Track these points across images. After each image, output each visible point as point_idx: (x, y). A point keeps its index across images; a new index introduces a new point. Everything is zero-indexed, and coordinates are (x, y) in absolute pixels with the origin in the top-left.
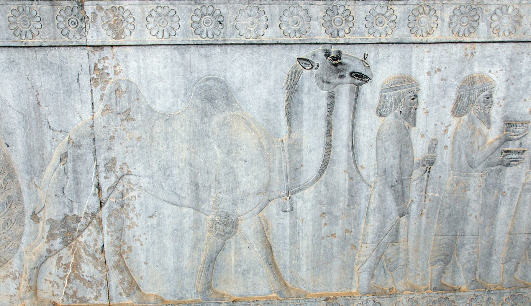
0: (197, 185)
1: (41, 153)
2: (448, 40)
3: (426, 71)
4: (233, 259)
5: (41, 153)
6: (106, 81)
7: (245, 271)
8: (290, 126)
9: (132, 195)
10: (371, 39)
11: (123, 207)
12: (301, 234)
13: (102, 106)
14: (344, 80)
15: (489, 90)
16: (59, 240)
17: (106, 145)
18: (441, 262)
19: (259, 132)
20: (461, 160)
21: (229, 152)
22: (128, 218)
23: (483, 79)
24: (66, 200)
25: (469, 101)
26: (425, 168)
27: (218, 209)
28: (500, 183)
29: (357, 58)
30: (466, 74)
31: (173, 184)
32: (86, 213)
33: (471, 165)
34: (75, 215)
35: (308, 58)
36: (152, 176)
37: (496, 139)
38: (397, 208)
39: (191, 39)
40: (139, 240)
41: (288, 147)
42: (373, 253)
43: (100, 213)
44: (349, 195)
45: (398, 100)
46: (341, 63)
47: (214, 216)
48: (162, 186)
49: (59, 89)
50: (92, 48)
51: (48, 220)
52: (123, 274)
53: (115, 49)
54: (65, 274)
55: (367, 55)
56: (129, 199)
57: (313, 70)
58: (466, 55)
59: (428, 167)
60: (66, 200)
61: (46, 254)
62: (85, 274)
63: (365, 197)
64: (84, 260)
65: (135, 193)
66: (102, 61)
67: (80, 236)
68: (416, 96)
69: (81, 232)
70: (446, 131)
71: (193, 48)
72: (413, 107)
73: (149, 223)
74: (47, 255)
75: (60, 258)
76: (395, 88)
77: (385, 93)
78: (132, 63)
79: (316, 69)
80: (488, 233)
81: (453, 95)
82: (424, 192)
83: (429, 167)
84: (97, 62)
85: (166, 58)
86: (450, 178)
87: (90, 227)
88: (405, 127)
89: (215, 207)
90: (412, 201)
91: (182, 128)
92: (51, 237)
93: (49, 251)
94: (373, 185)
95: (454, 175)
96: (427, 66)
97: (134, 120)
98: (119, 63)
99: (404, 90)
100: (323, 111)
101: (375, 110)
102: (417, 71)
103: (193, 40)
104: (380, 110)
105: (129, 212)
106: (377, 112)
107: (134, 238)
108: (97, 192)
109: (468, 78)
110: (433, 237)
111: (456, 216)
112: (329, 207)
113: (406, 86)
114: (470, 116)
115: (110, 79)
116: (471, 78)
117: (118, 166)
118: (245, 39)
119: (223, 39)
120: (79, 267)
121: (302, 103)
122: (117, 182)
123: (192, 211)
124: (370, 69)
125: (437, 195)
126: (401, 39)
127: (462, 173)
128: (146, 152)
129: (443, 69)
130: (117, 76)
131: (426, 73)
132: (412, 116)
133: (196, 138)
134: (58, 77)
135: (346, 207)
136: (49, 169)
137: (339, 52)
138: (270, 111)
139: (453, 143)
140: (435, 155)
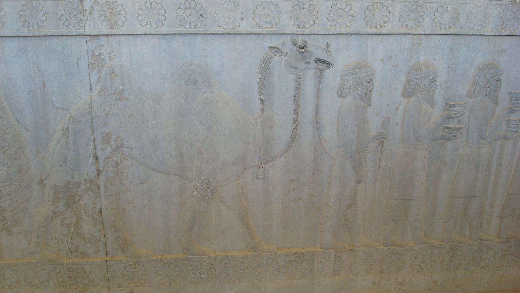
0: (182, 156)
2: (399, 32)
6: (102, 66)
8: (262, 105)
10: (332, 30)
11: (117, 175)
14: (310, 66)
15: (433, 75)
16: (62, 203)
18: (392, 222)
26: (379, 142)
27: (201, 177)
32: (85, 180)
34: (76, 181)
35: (278, 47)
37: (439, 117)
50: (90, 37)
53: (110, 38)
55: (330, 44)
58: (414, 45)
59: (381, 141)
64: (85, 220)
67: (81, 199)
68: (372, 80)
70: (397, 110)
71: (178, 38)
72: (369, 89)
75: (64, 219)
77: (345, 77)
79: (285, 56)
84: (94, 49)
88: (362, 106)
93: (54, 212)
97: (126, 99)
99: (360, 75)
103: (178, 31)
108: (95, 162)
115: (106, 64)
116: (418, 65)
120: (80, 226)
125: (389, 165)
126: (358, 30)
127: (411, 146)
130: (111, 61)
137: (305, 41)
140: (388, 131)
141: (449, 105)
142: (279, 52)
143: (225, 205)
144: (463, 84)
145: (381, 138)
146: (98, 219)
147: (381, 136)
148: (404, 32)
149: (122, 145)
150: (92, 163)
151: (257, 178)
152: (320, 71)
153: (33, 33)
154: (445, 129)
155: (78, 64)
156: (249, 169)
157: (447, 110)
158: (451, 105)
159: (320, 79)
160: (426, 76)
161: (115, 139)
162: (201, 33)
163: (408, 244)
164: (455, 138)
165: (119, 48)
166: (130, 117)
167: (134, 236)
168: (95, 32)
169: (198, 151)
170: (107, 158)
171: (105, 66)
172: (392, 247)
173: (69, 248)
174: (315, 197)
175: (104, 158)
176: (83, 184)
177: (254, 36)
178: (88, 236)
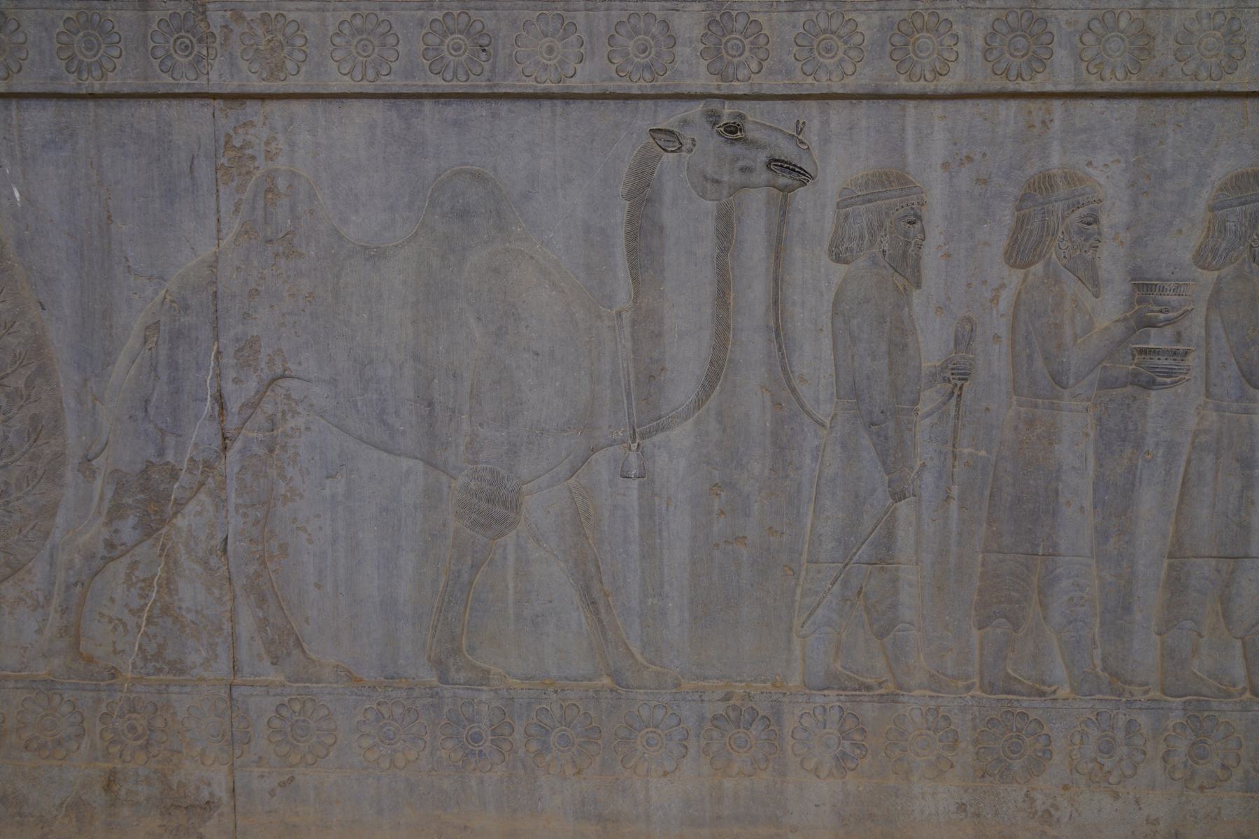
4: (511, 585)
7: (537, 616)
8: (635, 279)
10: (808, 84)
11: (271, 450)
12: (665, 534)
13: (236, 226)
15: (1091, 206)
16: (132, 520)
18: (1004, 620)
25: (1043, 228)
26: (949, 386)
27: (476, 462)
29: (781, 131)
31: (380, 400)
32: (191, 459)
33: (1058, 379)
34: (168, 463)
37: (1118, 321)
38: (887, 478)
39: (421, 83)
40: (305, 530)
42: (835, 586)
45: (875, 224)
46: (744, 140)
48: (356, 405)
49: (153, 188)
51: (111, 473)
54: (142, 602)
55: (804, 123)
57: (684, 153)
59: (956, 385)
61: (102, 551)
62: (184, 606)
65: (300, 422)
66: (240, 131)
68: (920, 218)
69: (180, 504)
70: (995, 299)
71: (428, 105)
75: (134, 565)
76: (869, 197)
79: (690, 151)
81: (1007, 215)
82: (950, 444)
83: (959, 385)
84: (231, 132)
87: (202, 496)
88: (897, 287)
90: (924, 465)
91: (401, 276)
92: (116, 512)
94: (827, 422)
97: (301, 255)
98: (276, 136)
100: (707, 248)
101: (826, 247)
104: (837, 247)
105: (285, 465)
106: (830, 251)
107: (295, 526)
108: (217, 413)
109: (1040, 177)
110: (981, 556)
113: (893, 193)
114: (1048, 264)
115: (258, 168)
116: (1045, 178)
118: (535, 83)
119: (488, 83)
120: (172, 587)
121: (662, 229)
122: (261, 394)
123: (420, 466)
124: (811, 154)
125: (983, 453)
127: (1040, 401)
130: (270, 162)
136: (122, 359)
137: (741, 116)
139: (1013, 329)
142: (674, 141)
143: (539, 545)
144: (1180, 231)
145: (954, 376)
146: (219, 568)
147: (953, 372)
148: (999, 87)
149: (287, 372)
150: (211, 416)
151: (625, 473)
152: (781, 193)
153: (87, 88)
154: (1137, 357)
155: (191, 167)
156: (602, 451)
157: (1140, 302)
158: (1150, 288)
159: (782, 212)
160: (1069, 208)
161: (269, 355)
162: (481, 91)
163: (1054, 692)
164: (1168, 380)
165: (289, 130)
166: (307, 299)
167: (307, 621)
168: (232, 87)
169: (471, 392)
171: (254, 174)
172: (1010, 697)
173: (140, 647)
174: (781, 536)
175: (240, 405)
176: (184, 471)
177: (612, 104)
178: (190, 617)
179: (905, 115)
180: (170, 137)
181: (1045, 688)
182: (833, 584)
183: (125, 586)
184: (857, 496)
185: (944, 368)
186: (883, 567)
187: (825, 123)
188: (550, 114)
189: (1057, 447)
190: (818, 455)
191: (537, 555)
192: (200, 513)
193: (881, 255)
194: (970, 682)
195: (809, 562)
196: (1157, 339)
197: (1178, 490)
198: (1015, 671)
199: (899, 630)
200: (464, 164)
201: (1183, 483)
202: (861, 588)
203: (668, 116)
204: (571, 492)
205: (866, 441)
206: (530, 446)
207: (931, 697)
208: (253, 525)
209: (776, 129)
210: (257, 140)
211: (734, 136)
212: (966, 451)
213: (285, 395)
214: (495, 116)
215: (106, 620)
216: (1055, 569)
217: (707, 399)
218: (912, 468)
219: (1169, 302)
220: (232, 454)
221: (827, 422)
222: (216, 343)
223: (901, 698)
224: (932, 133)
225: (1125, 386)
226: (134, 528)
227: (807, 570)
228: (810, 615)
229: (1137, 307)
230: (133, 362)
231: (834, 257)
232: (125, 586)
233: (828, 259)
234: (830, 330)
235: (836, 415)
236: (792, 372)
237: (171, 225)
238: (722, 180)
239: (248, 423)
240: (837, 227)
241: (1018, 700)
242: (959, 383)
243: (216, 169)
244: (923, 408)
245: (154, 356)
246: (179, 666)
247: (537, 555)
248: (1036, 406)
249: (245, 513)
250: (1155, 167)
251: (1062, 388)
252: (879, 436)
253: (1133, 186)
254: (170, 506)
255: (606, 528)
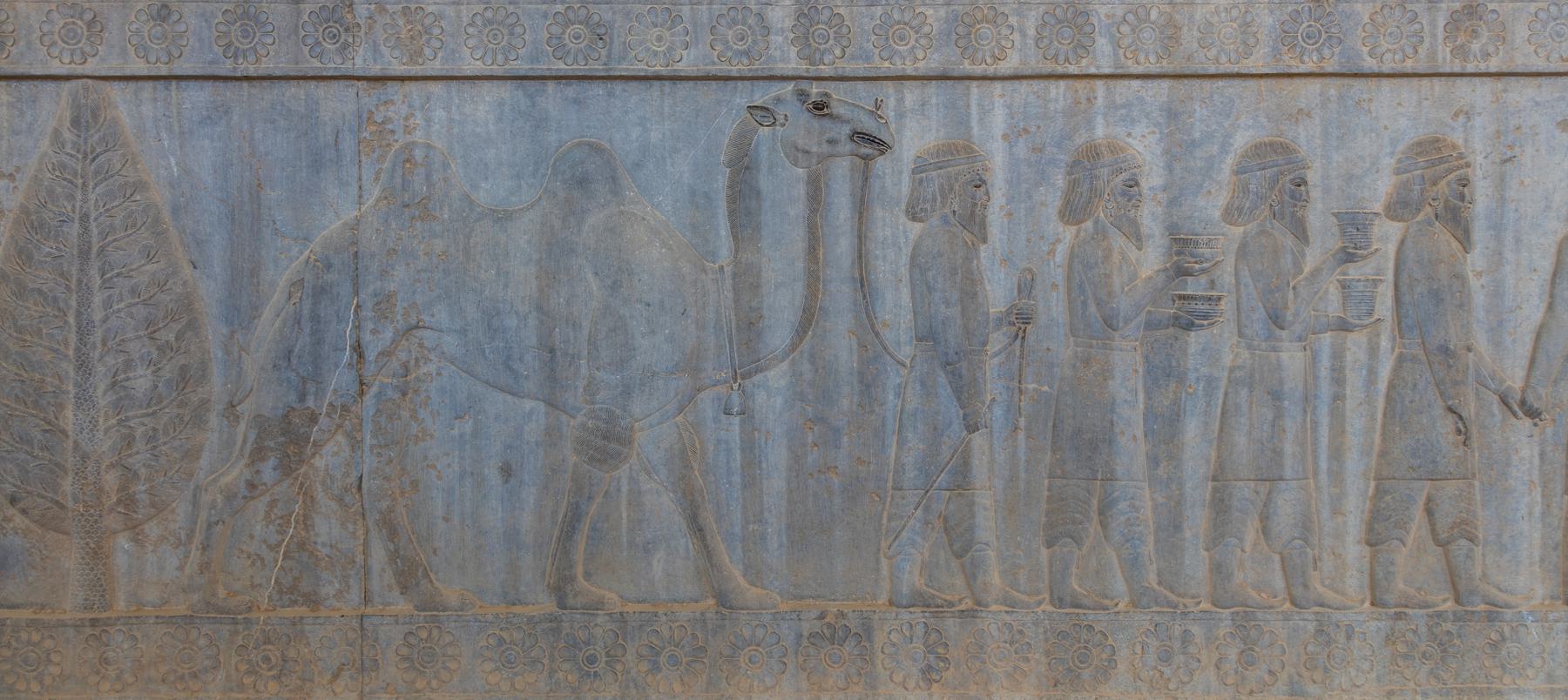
0: (552, 351)
1: (255, 281)
3: (1001, 133)
4: (624, 515)
5: (255, 281)
7: (649, 543)
8: (735, 237)
9: (425, 371)
11: (404, 394)
12: (764, 465)
13: (376, 192)
14: (840, 149)
15: (1132, 171)
16: (272, 462)
17: (378, 267)
18: (1070, 540)
19: (674, 248)
20: (1087, 313)
21: (615, 286)
22: (416, 419)
23: (1114, 148)
24: (293, 376)
25: (1091, 191)
26: (1014, 329)
27: (593, 403)
28: (1179, 366)
30: (1081, 139)
32: (331, 404)
33: (1110, 323)
34: (308, 408)
35: (766, 106)
36: (465, 330)
37: (1159, 271)
38: (962, 412)
40: (434, 467)
41: (734, 279)
43: (360, 406)
44: (861, 382)
46: (830, 116)
47: (585, 419)
48: (484, 352)
49: (301, 159)
51: (254, 417)
52: (396, 540)
55: (882, 100)
56: (418, 379)
57: (778, 128)
60: (293, 376)
61: (243, 491)
62: (319, 540)
63: (894, 388)
64: (321, 507)
65: (432, 368)
66: (382, 108)
67: (317, 455)
68: (984, 182)
70: (1052, 252)
71: (551, 86)
73: (456, 432)
74: (246, 493)
76: (939, 164)
78: (437, 113)
80: (1166, 476)
81: (1060, 180)
82: (1016, 380)
84: (374, 110)
85: (501, 104)
86: (1069, 352)
87: (340, 437)
89: (588, 398)
90: (993, 400)
92: (258, 454)
94: (908, 362)
95: (1077, 345)
96: (998, 121)
97: (435, 218)
100: (798, 209)
101: (903, 207)
102: (983, 132)
104: (913, 208)
106: (907, 212)
107: (425, 464)
108: (355, 362)
109: (1087, 147)
111: (1089, 436)
112: (820, 408)
113: (962, 161)
114: (1096, 222)
117: (399, 309)
120: (308, 523)
121: (758, 193)
123: (542, 407)
124: (888, 128)
127: (1094, 342)
128: (456, 283)
129: (1033, 129)
130: (409, 136)
131: (1000, 138)
132: (977, 220)
133: (553, 257)
134: (300, 137)
135: (854, 407)
136: (267, 313)
137: (826, 94)
138: (697, 207)
139: (1069, 279)
141: (1181, 244)
144: (1209, 192)
146: (353, 505)
150: (349, 364)
155: (336, 141)
156: (707, 391)
158: (1186, 242)
160: (1113, 173)
164: (1205, 322)
167: (435, 552)
169: (589, 340)
170: (386, 354)
172: (1077, 611)
178: (326, 551)
179: (969, 94)
180: (318, 114)
181: (1107, 602)
182: (916, 509)
183: (264, 523)
184: (935, 429)
185: (1009, 313)
186: (960, 493)
187: (901, 101)
188: (659, 93)
189: (1110, 382)
190: (900, 393)
191: (649, 486)
192: (336, 454)
193: (951, 215)
194: (1041, 597)
195: (894, 489)
196: (1193, 287)
197: (1218, 420)
198: (1080, 586)
199: (976, 551)
200: (583, 137)
201: (1223, 414)
202: (941, 513)
203: (762, 95)
204: (678, 428)
205: (942, 379)
206: (643, 388)
207: (1007, 612)
208: (387, 464)
209: (858, 106)
210: (397, 117)
211: (821, 113)
212: (1031, 386)
213: (419, 344)
214: (610, 94)
215: (245, 556)
216: (1113, 492)
217: (801, 342)
218: (984, 403)
219: (1203, 254)
220: (369, 399)
221: (908, 362)
222: (356, 298)
223: (980, 614)
224: (993, 109)
225: (1168, 328)
226: (274, 469)
227: (892, 496)
228: (896, 537)
229: (1175, 258)
230: (278, 316)
231: (910, 217)
232: (264, 523)
233: (905, 219)
234: (908, 281)
235: (915, 355)
236: (876, 318)
237: (316, 192)
238: (812, 150)
239: (384, 369)
240: (913, 191)
241: (1084, 614)
242: (1023, 326)
243: (359, 142)
244: (992, 348)
245: (298, 310)
246: (313, 598)
247: (649, 486)
248: (1091, 347)
249: (379, 453)
250: (1185, 138)
251: (1113, 330)
252: (954, 375)
253: (1167, 153)
254: (309, 448)
255: (711, 461)
